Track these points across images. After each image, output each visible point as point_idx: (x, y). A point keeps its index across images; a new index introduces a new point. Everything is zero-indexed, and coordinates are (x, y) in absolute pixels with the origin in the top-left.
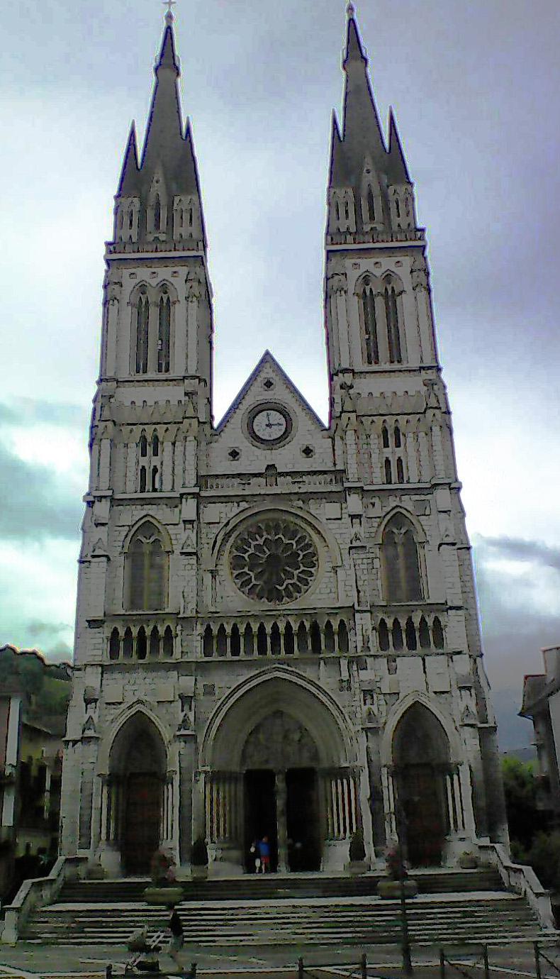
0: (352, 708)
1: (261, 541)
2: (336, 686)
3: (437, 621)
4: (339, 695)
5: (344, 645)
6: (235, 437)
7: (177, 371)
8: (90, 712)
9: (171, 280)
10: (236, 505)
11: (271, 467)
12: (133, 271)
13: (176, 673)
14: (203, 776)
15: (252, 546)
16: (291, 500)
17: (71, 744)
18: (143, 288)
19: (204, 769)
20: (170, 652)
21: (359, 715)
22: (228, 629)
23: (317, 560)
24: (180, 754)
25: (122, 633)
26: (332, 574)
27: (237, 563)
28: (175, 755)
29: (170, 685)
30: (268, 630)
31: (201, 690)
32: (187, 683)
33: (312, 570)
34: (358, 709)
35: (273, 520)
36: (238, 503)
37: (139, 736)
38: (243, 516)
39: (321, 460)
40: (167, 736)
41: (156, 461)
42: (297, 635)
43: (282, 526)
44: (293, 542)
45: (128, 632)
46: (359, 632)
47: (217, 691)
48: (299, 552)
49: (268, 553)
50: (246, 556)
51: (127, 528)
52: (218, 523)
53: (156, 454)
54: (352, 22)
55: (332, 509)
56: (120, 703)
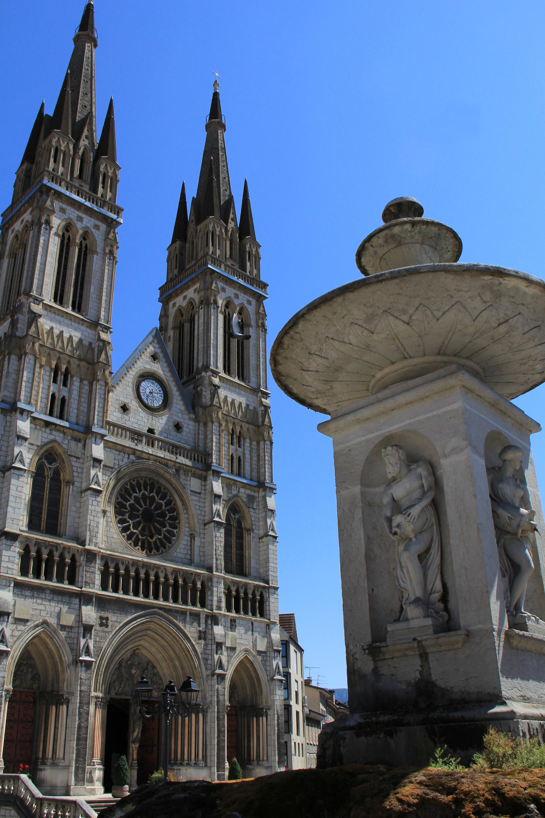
1: (139, 495)
2: (196, 635)
3: (261, 595)
4: (197, 644)
9: (94, 230)
10: (127, 456)
11: (151, 431)
12: (64, 206)
13: (77, 601)
14: (93, 701)
15: (133, 497)
18: (68, 227)
19: (95, 694)
21: (210, 662)
23: (179, 523)
26: (189, 539)
31: (98, 622)
32: (90, 613)
34: (210, 656)
36: (129, 455)
40: (67, 659)
42: (172, 586)
43: (156, 486)
46: (215, 594)
47: (110, 623)
48: (167, 512)
49: (144, 507)
52: (112, 468)
54: (216, 96)
55: (194, 484)
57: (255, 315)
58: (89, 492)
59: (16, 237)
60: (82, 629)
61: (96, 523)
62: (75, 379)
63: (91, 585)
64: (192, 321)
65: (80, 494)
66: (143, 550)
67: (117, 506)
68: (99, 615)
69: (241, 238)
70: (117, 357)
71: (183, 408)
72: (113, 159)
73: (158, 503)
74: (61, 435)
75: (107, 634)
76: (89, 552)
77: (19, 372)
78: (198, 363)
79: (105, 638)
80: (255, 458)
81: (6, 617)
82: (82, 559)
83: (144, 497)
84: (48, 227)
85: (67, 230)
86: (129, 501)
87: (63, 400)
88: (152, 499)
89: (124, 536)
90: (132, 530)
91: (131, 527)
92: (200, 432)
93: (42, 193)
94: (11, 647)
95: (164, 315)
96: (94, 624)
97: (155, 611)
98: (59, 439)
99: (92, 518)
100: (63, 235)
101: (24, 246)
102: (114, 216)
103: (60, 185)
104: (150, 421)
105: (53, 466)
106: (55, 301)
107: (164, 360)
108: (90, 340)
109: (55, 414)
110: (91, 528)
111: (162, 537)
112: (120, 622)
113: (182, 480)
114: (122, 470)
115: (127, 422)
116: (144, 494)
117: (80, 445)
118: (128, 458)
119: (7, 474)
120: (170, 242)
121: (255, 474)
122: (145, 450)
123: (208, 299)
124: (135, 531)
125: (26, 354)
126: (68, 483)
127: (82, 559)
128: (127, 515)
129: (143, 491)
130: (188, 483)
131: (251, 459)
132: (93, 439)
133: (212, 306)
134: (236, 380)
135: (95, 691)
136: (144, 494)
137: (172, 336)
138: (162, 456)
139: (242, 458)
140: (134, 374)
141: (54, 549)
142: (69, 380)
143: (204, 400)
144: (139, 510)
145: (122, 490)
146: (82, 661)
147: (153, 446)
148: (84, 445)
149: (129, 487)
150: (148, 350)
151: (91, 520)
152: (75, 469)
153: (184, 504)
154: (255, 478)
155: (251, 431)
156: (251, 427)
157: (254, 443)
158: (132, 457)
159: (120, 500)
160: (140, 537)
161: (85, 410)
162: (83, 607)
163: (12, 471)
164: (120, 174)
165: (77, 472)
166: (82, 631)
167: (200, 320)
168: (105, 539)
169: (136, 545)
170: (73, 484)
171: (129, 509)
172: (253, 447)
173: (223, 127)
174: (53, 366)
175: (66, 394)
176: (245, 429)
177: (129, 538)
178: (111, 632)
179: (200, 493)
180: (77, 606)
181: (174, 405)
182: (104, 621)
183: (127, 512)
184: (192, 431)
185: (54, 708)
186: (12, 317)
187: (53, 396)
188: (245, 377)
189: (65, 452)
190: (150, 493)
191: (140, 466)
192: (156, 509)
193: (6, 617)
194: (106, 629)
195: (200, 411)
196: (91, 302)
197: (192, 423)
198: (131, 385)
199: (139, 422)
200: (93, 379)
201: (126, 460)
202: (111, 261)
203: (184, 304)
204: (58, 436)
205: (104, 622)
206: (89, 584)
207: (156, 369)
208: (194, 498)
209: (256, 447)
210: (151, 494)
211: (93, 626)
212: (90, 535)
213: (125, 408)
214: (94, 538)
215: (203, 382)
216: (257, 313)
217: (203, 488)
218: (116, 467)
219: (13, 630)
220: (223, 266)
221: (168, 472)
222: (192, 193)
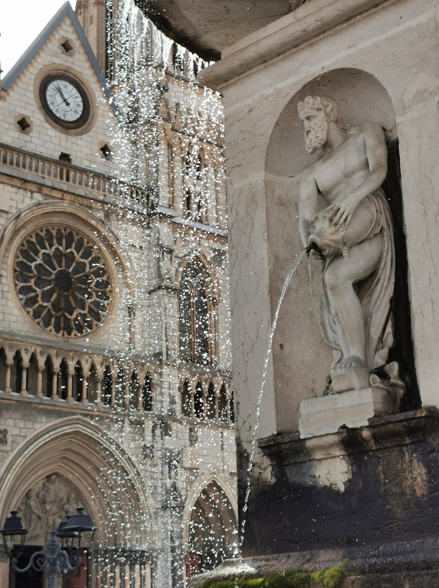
0: (152, 481)
5: (148, 406)
10: (29, 194)
11: (65, 157)
15: (40, 255)
27: (22, 272)
30: (71, 370)
36: (32, 192)
43: (76, 238)
44: (87, 262)
47: (9, 439)
49: (58, 269)
52: (7, 212)
66: (58, 331)
67: (18, 269)
73: (78, 263)
75: (5, 454)
83: (58, 255)
86: (35, 260)
88: (70, 258)
89: (28, 312)
90: (41, 302)
91: (39, 299)
97: (78, 419)
107: (82, 50)
112: (25, 437)
114: (22, 215)
116: (57, 249)
118: (32, 198)
122: (56, 186)
124: (45, 304)
128: (33, 281)
129: (56, 246)
136: (57, 249)
137: (95, 15)
140: (36, 72)
144: (51, 274)
145: (23, 245)
147: (68, 180)
149: (34, 240)
150: (57, 36)
158: (38, 197)
159: (21, 259)
160: (53, 313)
169: (47, 324)
171: (35, 272)
177: (36, 315)
178: (12, 451)
183: (32, 277)
190: (67, 249)
191: (50, 209)
192: (76, 271)
198: (31, 88)
199: (48, 145)
207: (70, 65)
210: (69, 250)
213: (23, 125)
221: (94, 218)
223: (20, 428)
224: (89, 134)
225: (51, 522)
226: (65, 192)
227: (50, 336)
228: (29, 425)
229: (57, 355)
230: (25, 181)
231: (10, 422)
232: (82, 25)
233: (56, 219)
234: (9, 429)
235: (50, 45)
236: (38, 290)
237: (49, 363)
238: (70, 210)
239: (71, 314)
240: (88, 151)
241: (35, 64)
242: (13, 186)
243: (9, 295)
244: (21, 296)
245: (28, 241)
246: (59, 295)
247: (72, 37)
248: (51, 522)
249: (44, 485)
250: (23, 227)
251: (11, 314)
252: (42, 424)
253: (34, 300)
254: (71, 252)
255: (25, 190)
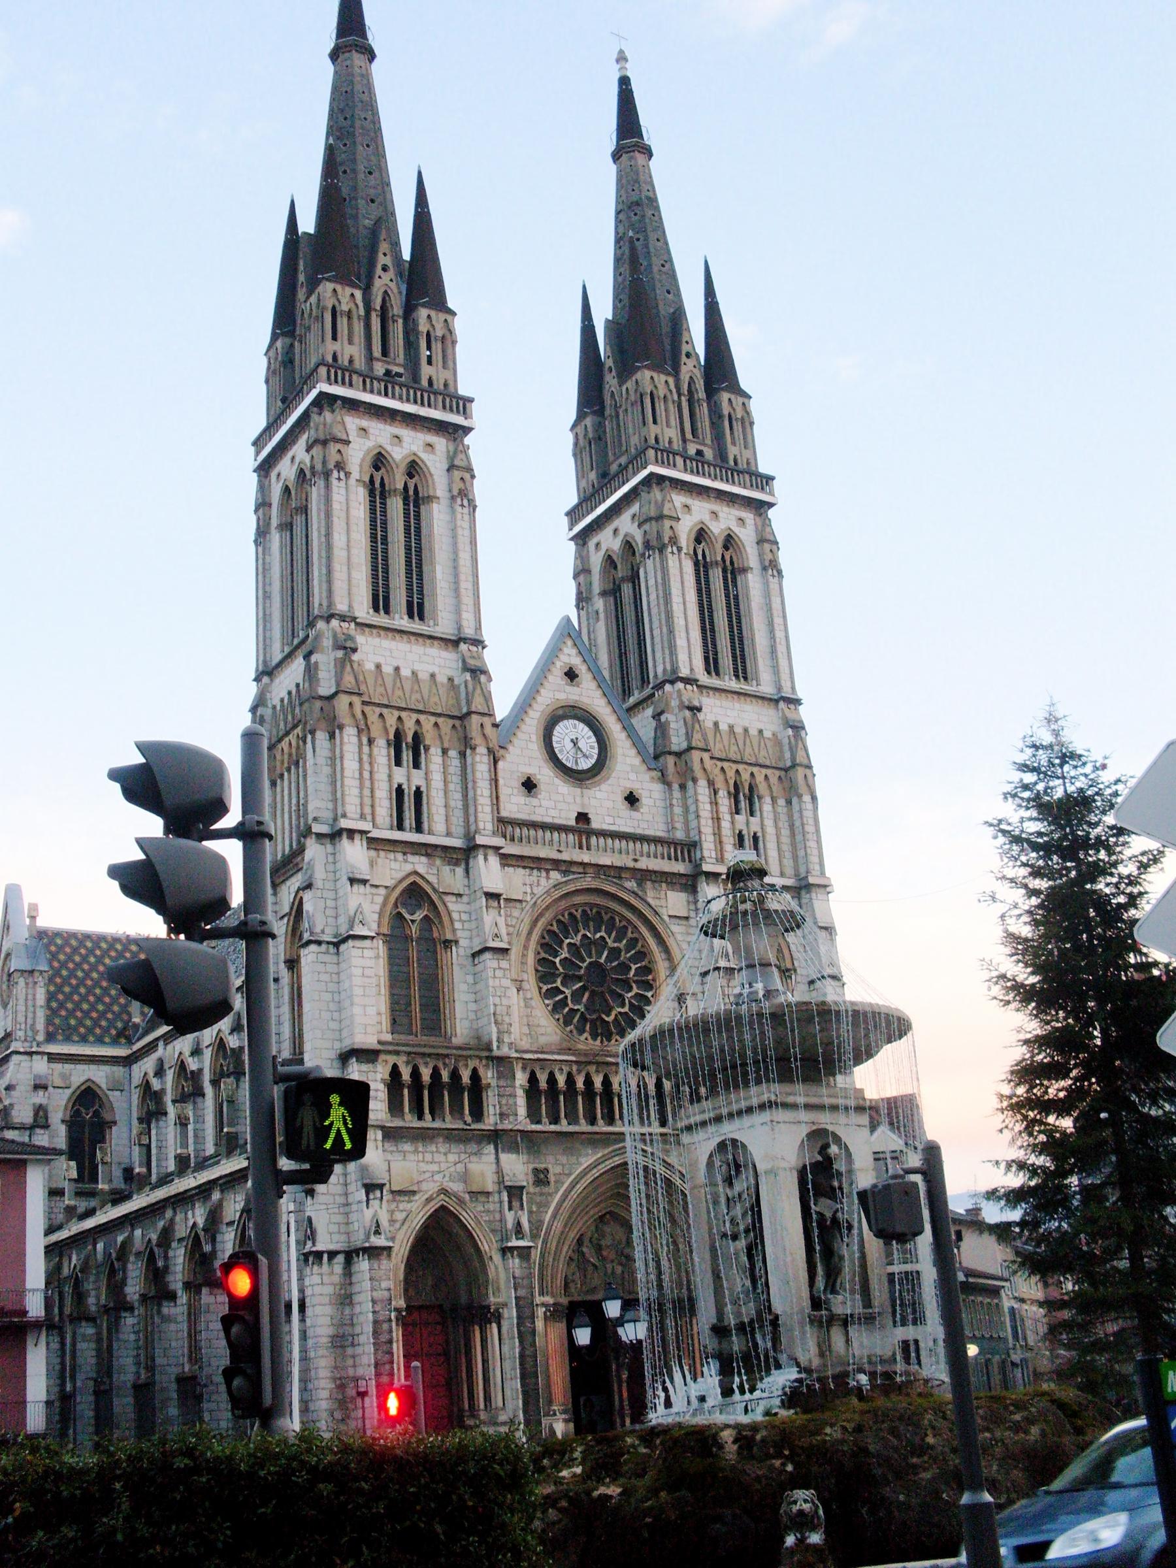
1: (577, 939)
6: (525, 755)
7: (444, 625)
8: (375, 1204)
9: (423, 456)
10: (544, 874)
11: (583, 817)
12: (365, 423)
15: (565, 946)
16: (620, 878)
17: (325, 1256)
18: (379, 461)
20: (478, 1113)
22: (561, 1080)
23: (654, 980)
24: (514, 1278)
25: (406, 1075)
27: (545, 972)
28: (503, 1281)
29: (484, 1166)
31: (531, 1179)
32: (517, 1167)
33: (649, 994)
35: (592, 906)
36: (548, 871)
37: (441, 1247)
38: (557, 894)
39: (650, 819)
41: (418, 779)
43: (606, 918)
45: (416, 1074)
47: (552, 1178)
49: (588, 960)
50: (557, 960)
51: (382, 891)
52: (520, 901)
53: (416, 765)
55: (674, 902)
56: (414, 1193)
57: (755, 545)
58: (487, 956)
59: (287, 490)
60: (505, 1195)
61: (505, 1009)
62: (432, 750)
63: (511, 1118)
64: (634, 578)
65: (470, 959)
68: (531, 1166)
69: (711, 392)
70: (504, 698)
71: (637, 761)
72: (439, 303)
74: (424, 859)
76: (501, 1060)
77: (335, 760)
78: (655, 667)
79: (547, 1205)
80: (785, 832)
81: (378, 1193)
82: (490, 1074)
84: (342, 475)
85: (377, 468)
87: (418, 793)
92: (675, 802)
93: (321, 409)
94: (393, 1239)
95: (582, 571)
96: (525, 1184)
98: (421, 870)
99: (497, 1001)
100: (372, 476)
101: (304, 510)
102: (458, 419)
103: (351, 385)
104: (578, 800)
105: (419, 916)
106: (376, 609)
108: (450, 673)
109: (407, 824)
110: (499, 1018)
111: (626, 1009)
112: (570, 1174)
113: (650, 900)
115: (537, 810)
116: (584, 936)
117: (460, 871)
118: (548, 878)
119: (343, 947)
120: (573, 416)
121: (788, 863)
123: (659, 536)
125: (341, 727)
126: (447, 944)
127: (488, 1076)
128: (559, 980)
130: (663, 902)
131: (778, 836)
132: (481, 858)
133: (669, 549)
134: (733, 685)
135: (542, 1293)
137: (601, 610)
138: (609, 863)
139: (759, 834)
141: (441, 1065)
142: (423, 756)
143: (674, 740)
146: (512, 1249)
147: (588, 849)
148: (467, 871)
149: (555, 928)
150: (558, 664)
151: (495, 1005)
152: (455, 916)
153: (661, 942)
154: (789, 871)
155: (774, 780)
156: (769, 772)
157: (781, 802)
158: (555, 876)
161: (460, 804)
162: (504, 1157)
163: (350, 943)
164: (458, 324)
165: (460, 920)
166: (506, 1199)
167: (649, 571)
168: (526, 1030)
169: (581, 1031)
170: (457, 942)
172: (780, 810)
173: (648, 152)
174: (392, 737)
175: (422, 783)
176: (760, 778)
177: (567, 1021)
178: (556, 1192)
179: (687, 918)
180: (493, 1157)
181: (620, 759)
182: (542, 1176)
184: (660, 803)
185: (477, 1328)
186: (307, 657)
187: (400, 791)
188: (749, 676)
189: (434, 889)
190: (595, 933)
191: (571, 887)
193: (378, 1193)
194: (546, 1190)
195: (671, 760)
196: (440, 598)
197: (658, 787)
198: (534, 738)
199: (561, 806)
200: (466, 745)
201: (543, 881)
202: (466, 510)
203: (616, 545)
204: (419, 864)
205: (541, 1177)
206: (508, 1116)
207: (577, 698)
208: (676, 928)
209: (785, 810)
210: (598, 935)
211: (523, 1187)
212: (499, 1032)
213: (529, 785)
214: (506, 1035)
215: (667, 704)
216: (761, 541)
217: (692, 907)
218: (528, 898)
219: (392, 1212)
220: (679, 461)
222: (603, 311)
223: (563, 1165)
224: (609, 782)
225: (609, 1271)
226: (586, 864)
227: (586, 1043)
228: (573, 1159)
229: (597, 1071)
230: (539, 859)
231: (551, 1158)
232: (587, 643)
233: (578, 899)
234: (550, 1166)
235: (550, 678)
236: (568, 992)
237: (589, 1082)
238: (595, 884)
239: (608, 1016)
240: (610, 804)
241: (535, 705)
242: (524, 867)
243: (533, 1003)
244: (547, 1002)
245: (549, 932)
246: (593, 993)
247: (576, 661)
248: (609, 1271)
249: (597, 1227)
250: (541, 915)
251: (539, 1026)
252: (588, 1158)
253: (563, 1002)
254: (602, 938)
255: (539, 869)
